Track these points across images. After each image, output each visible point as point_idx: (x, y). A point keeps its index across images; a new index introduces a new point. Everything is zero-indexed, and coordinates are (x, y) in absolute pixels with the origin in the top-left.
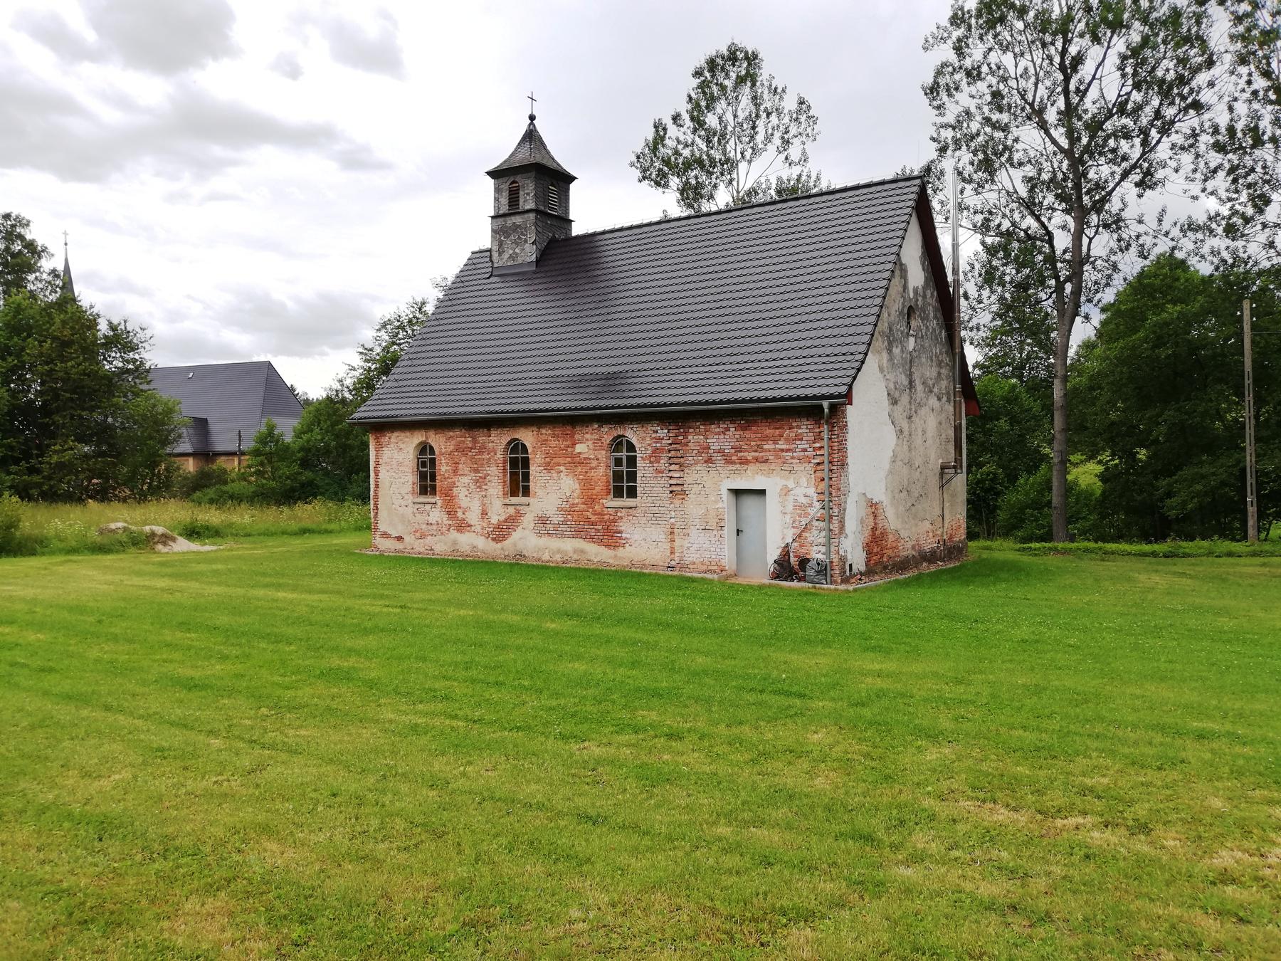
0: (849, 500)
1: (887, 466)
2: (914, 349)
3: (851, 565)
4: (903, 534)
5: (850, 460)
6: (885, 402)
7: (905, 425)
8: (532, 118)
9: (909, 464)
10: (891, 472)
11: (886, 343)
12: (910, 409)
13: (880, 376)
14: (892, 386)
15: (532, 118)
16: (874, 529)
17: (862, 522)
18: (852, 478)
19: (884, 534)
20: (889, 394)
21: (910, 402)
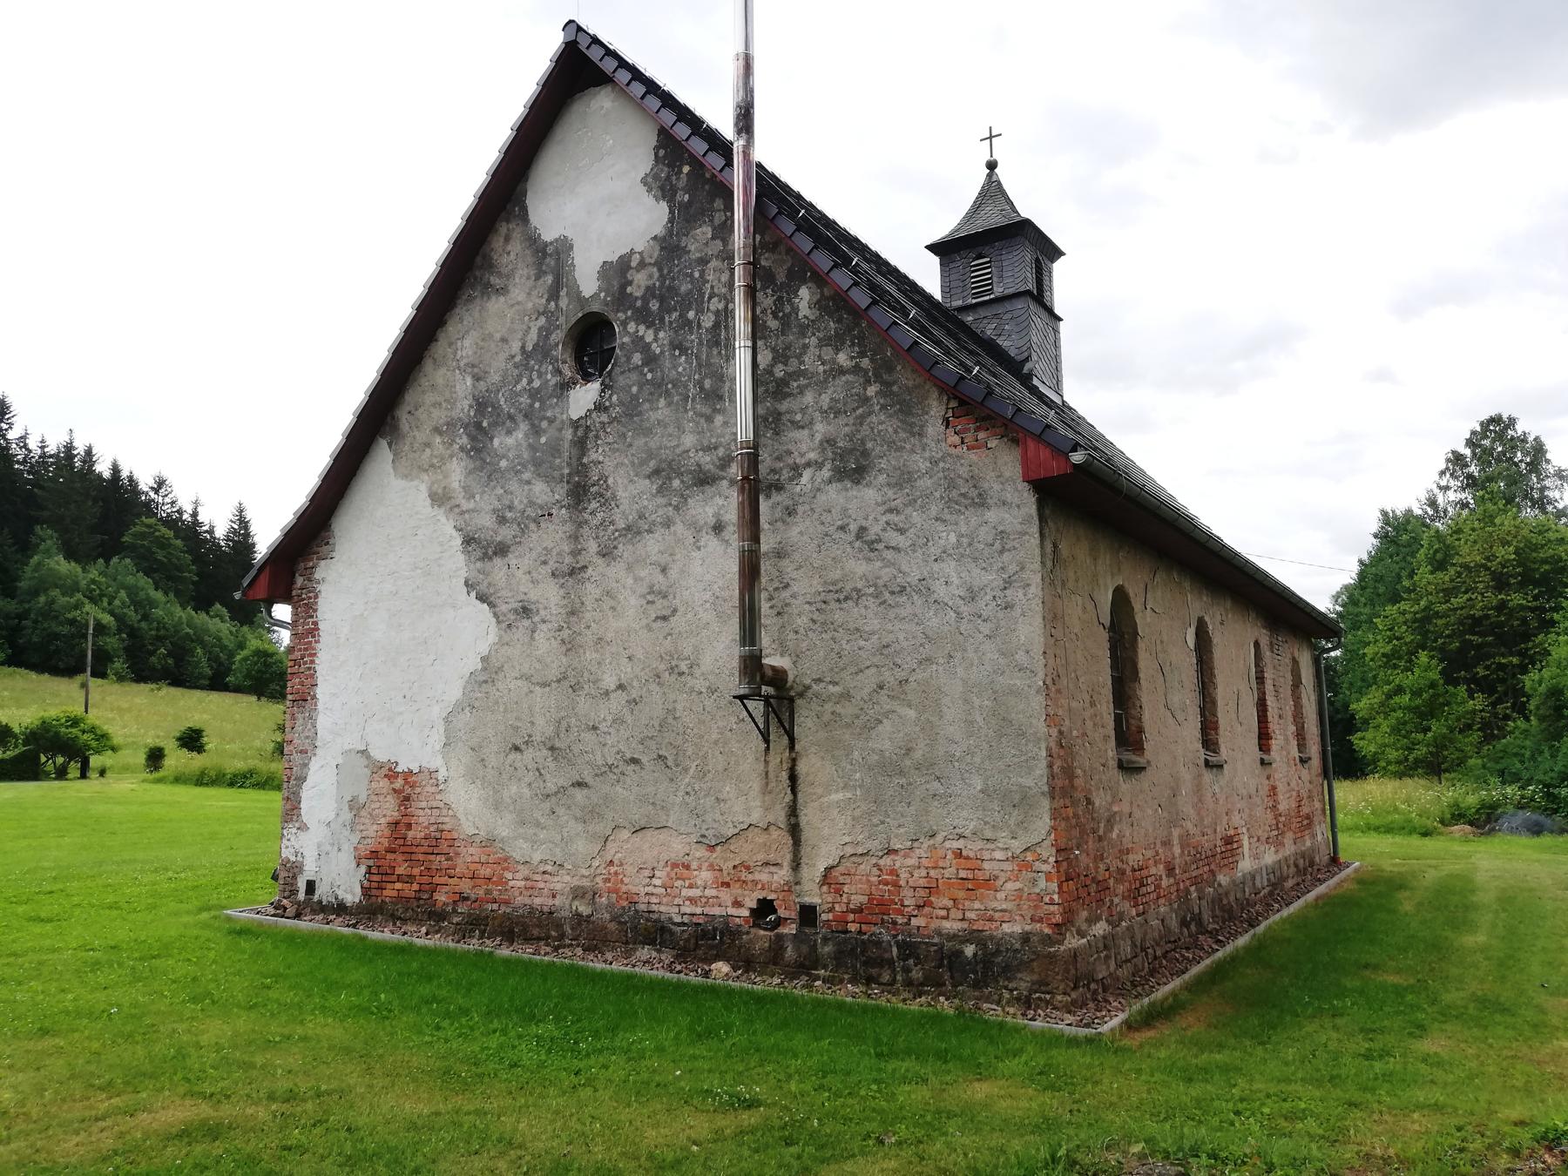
0: (314, 765)
1: (455, 692)
2: (599, 407)
3: (311, 887)
4: (519, 850)
5: (321, 692)
6: (457, 563)
7: (549, 596)
8: (992, 166)
9: (571, 682)
10: (467, 704)
11: (465, 440)
12: (576, 553)
13: (440, 513)
14: (486, 521)
15: (992, 166)
16: (398, 827)
17: (355, 806)
18: (324, 721)
19: (440, 842)
20: (468, 541)
21: (575, 538)
